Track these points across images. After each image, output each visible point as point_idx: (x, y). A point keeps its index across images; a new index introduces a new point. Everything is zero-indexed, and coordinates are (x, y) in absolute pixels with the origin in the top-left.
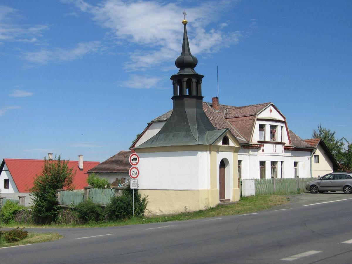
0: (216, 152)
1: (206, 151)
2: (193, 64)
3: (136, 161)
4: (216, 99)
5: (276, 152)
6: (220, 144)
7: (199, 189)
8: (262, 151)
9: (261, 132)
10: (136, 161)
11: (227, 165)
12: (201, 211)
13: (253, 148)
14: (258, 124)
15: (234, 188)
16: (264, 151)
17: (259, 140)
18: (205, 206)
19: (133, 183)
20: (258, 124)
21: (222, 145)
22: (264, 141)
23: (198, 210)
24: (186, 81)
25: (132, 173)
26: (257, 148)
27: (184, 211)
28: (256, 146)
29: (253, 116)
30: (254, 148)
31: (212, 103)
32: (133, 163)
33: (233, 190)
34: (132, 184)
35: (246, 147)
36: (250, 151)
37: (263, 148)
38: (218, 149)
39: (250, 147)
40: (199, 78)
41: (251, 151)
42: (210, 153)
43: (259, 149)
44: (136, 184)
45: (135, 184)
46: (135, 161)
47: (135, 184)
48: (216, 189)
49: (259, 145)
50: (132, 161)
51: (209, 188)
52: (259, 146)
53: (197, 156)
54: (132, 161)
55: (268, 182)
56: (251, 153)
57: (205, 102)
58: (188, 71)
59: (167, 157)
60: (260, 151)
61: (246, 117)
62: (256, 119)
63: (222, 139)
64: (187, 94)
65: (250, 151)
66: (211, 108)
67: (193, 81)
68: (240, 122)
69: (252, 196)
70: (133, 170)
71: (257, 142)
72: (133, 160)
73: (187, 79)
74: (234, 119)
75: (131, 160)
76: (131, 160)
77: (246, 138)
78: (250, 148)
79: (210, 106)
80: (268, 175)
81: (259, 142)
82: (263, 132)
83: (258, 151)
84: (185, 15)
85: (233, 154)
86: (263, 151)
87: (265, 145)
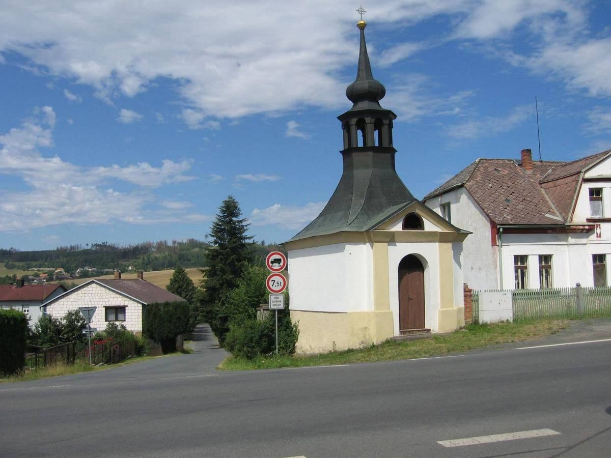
0: (387, 244)
1: (365, 243)
2: (377, 93)
3: (279, 264)
4: (527, 152)
5: (602, 238)
6: (398, 227)
7: (348, 311)
8: (597, 237)
9: (592, 202)
10: (279, 264)
11: (426, 267)
12: (350, 351)
13: (575, 233)
14: (586, 188)
15: (442, 307)
16: (600, 236)
17: (589, 216)
18: (362, 342)
19: (274, 300)
20: (586, 188)
21: (403, 229)
22: (602, 218)
23: (346, 349)
24: (355, 123)
25: (271, 283)
26: (585, 231)
27: (331, 349)
28: (582, 227)
29: (577, 175)
30: (576, 232)
31: (521, 159)
32: (272, 267)
33: (439, 311)
34: (273, 302)
35: (561, 230)
36: (570, 238)
37: (598, 231)
38: (392, 239)
39: (568, 231)
40: (389, 115)
41: (572, 238)
42: (372, 247)
43: (590, 232)
44: (280, 302)
45: (277, 302)
46: (277, 264)
47: (277, 302)
48: (451, 309)
49: (588, 225)
50: (271, 265)
51: (372, 309)
52: (587, 227)
53: (345, 252)
54: (271, 265)
55: (531, 295)
56: (571, 240)
57: (510, 160)
58: (364, 105)
59: (337, 252)
60: (593, 237)
61: (567, 178)
62: (581, 180)
63: (403, 218)
64: (377, 144)
65: (570, 238)
66: (519, 169)
67: (384, 123)
68: (558, 188)
69: (502, 322)
70: (273, 278)
71: (585, 221)
72: (272, 262)
73: (356, 119)
74: (551, 184)
75: (282, 259)
76: (270, 262)
77: (564, 215)
78: (568, 233)
79: (519, 165)
80: (533, 281)
81: (589, 220)
82: (600, 202)
83: (588, 237)
84: (361, 14)
85: (440, 247)
86: (599, 236)
87: (603, 225)
